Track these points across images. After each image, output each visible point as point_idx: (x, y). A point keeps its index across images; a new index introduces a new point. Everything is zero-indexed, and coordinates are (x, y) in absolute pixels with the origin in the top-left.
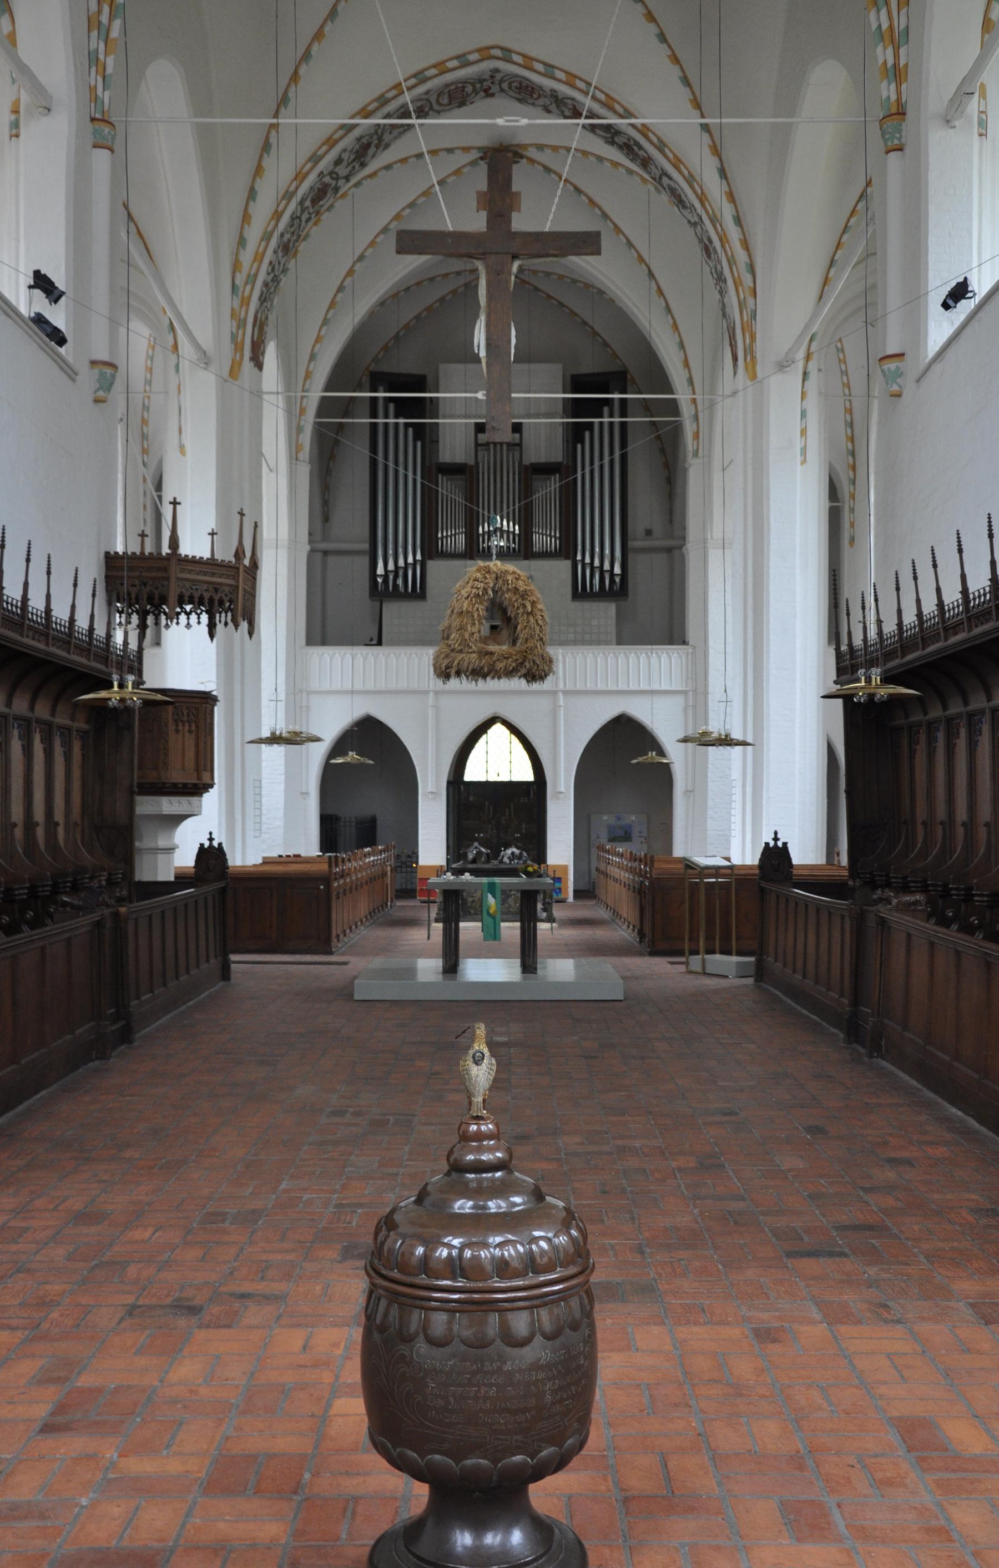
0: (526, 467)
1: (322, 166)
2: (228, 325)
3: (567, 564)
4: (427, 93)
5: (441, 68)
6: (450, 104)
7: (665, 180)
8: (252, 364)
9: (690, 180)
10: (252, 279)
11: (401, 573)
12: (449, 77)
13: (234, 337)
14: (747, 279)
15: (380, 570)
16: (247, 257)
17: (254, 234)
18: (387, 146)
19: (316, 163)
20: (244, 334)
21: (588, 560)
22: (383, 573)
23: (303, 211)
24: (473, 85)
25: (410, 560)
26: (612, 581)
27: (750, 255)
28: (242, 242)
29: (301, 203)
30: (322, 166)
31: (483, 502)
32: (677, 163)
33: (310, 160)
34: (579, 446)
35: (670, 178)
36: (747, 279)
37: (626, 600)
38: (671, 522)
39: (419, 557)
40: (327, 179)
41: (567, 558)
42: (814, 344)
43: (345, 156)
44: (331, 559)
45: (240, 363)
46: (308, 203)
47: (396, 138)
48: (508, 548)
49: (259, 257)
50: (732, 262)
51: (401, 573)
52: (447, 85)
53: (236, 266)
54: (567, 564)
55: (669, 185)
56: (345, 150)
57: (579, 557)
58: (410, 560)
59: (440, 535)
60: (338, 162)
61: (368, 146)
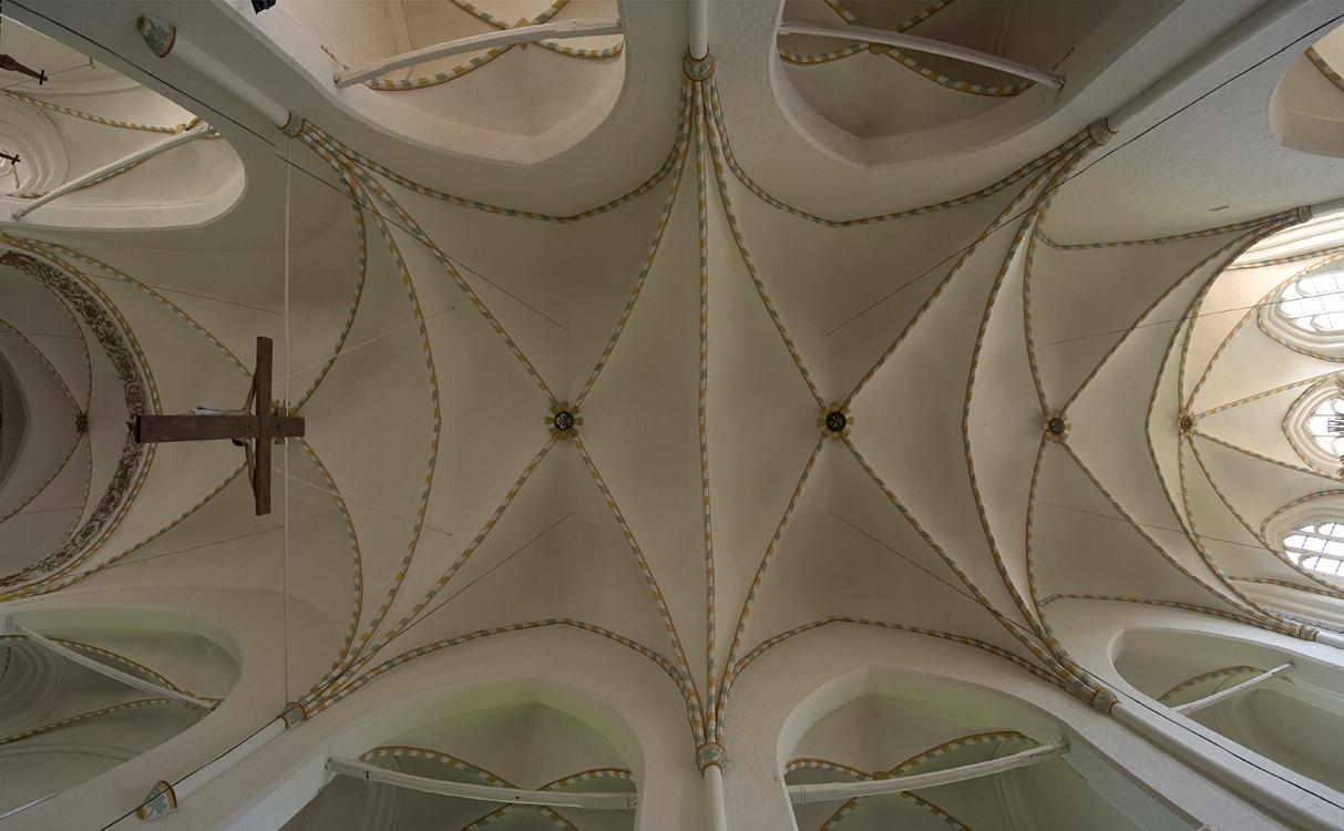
1: (110, 313)
2: (32, 237)
4: (141, 380)
5: (154, 389)
6: (130, 393)
7: (98, 524)
8: (6, 253)
9: (103, 540)
10: (55, 259)
12: (148, 392)
13: (25, 240)
14: (56, 585)
16: (69, 258)
17: (80, 265)
18: (109, 355)
19: (112, 311)
20: (25, 249)
23: (84, 300)
24: (141, 407)
27: (68, 585)
28: (78, 256)
29: (91, 299)
30: (110, 313)
32: (111, 531)
33: (114, 307)
35: (100, 527)
36: (56, 585)
40: (100, 316)
42: (21, 639)
43: (112, 329)
45: (9, 243)
46: (88, 303)
47: (114, 362)
49: (66, 266)
50: (63, 573)
52: (143, 392)
53: (65, 249)
55: (94, 526)
56: (115, 329)
60: (109, 324)
61: (114, 344)
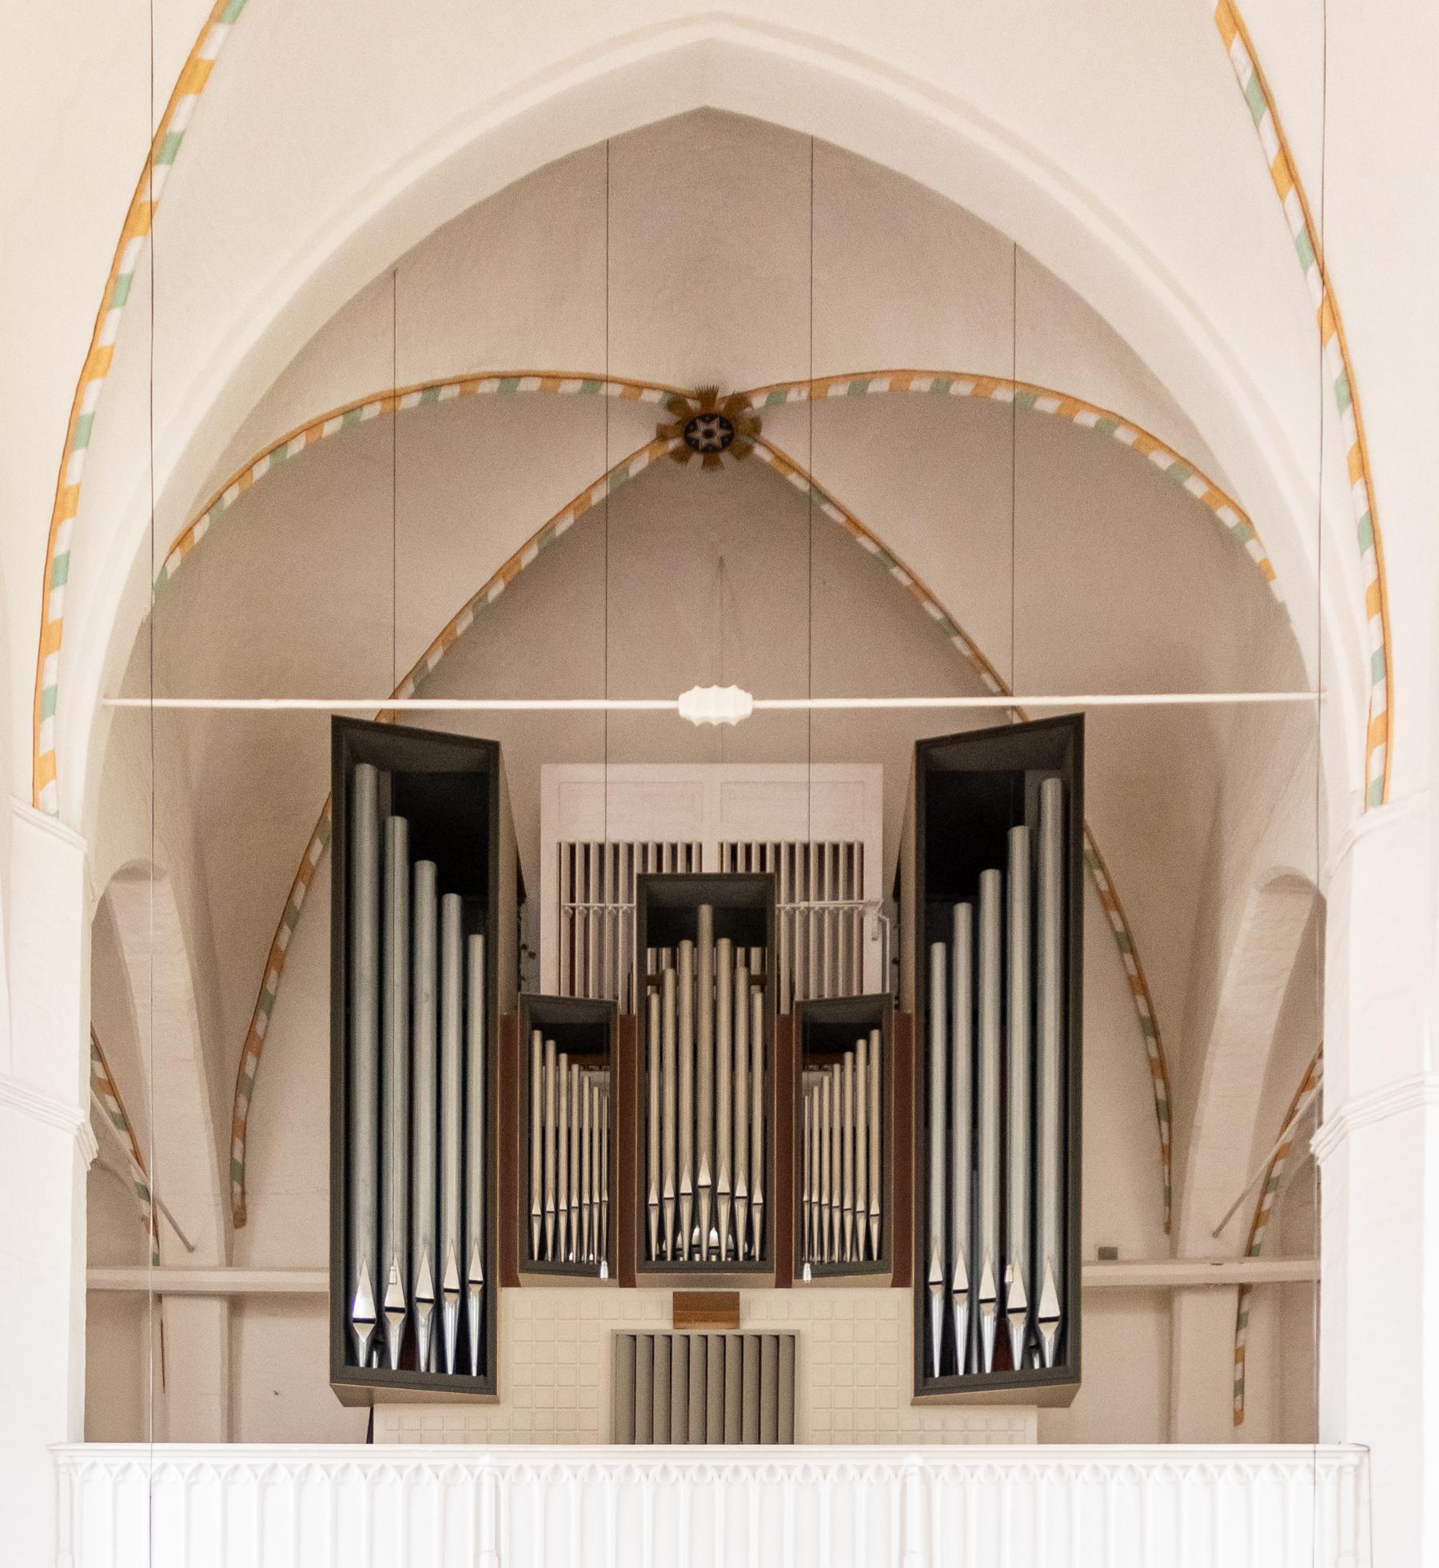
0: (786, 1021)
3: (905, 1297)
11: (424, 1314)
15: (363, 1307)
21: (960, 1281)
22: (372, 1315)
25: (451, 1280)
26: (1033, 1345)
31: (661, 1089)
34: (938, 950)
37: (1065, 1402)
38: (1168, 1228)
39: (475, 1273)
41: (900, 1282)
44: (254, 1326)
48: (733, 1252)
51: (424, 1314)
54: (905, 1297)
57: (936, 1274)
58: (451, 1280)
59: (536, 1210)
